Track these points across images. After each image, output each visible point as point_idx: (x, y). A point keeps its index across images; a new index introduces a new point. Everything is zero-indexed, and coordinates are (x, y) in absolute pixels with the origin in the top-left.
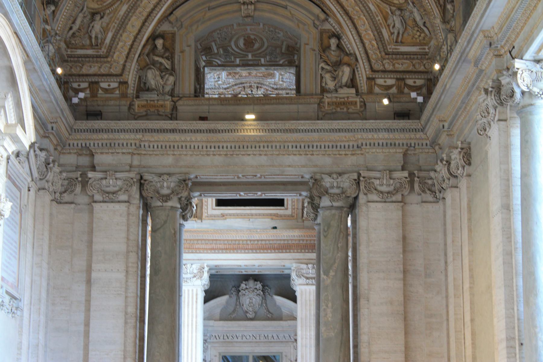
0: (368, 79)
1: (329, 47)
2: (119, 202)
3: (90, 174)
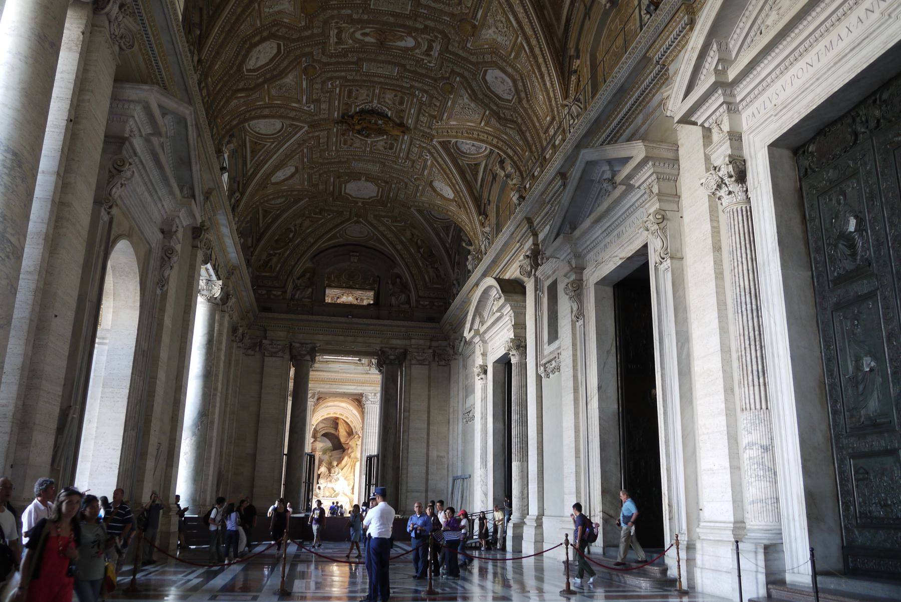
0: (416, 301)
2: (278, 357)
3: (264, 341)
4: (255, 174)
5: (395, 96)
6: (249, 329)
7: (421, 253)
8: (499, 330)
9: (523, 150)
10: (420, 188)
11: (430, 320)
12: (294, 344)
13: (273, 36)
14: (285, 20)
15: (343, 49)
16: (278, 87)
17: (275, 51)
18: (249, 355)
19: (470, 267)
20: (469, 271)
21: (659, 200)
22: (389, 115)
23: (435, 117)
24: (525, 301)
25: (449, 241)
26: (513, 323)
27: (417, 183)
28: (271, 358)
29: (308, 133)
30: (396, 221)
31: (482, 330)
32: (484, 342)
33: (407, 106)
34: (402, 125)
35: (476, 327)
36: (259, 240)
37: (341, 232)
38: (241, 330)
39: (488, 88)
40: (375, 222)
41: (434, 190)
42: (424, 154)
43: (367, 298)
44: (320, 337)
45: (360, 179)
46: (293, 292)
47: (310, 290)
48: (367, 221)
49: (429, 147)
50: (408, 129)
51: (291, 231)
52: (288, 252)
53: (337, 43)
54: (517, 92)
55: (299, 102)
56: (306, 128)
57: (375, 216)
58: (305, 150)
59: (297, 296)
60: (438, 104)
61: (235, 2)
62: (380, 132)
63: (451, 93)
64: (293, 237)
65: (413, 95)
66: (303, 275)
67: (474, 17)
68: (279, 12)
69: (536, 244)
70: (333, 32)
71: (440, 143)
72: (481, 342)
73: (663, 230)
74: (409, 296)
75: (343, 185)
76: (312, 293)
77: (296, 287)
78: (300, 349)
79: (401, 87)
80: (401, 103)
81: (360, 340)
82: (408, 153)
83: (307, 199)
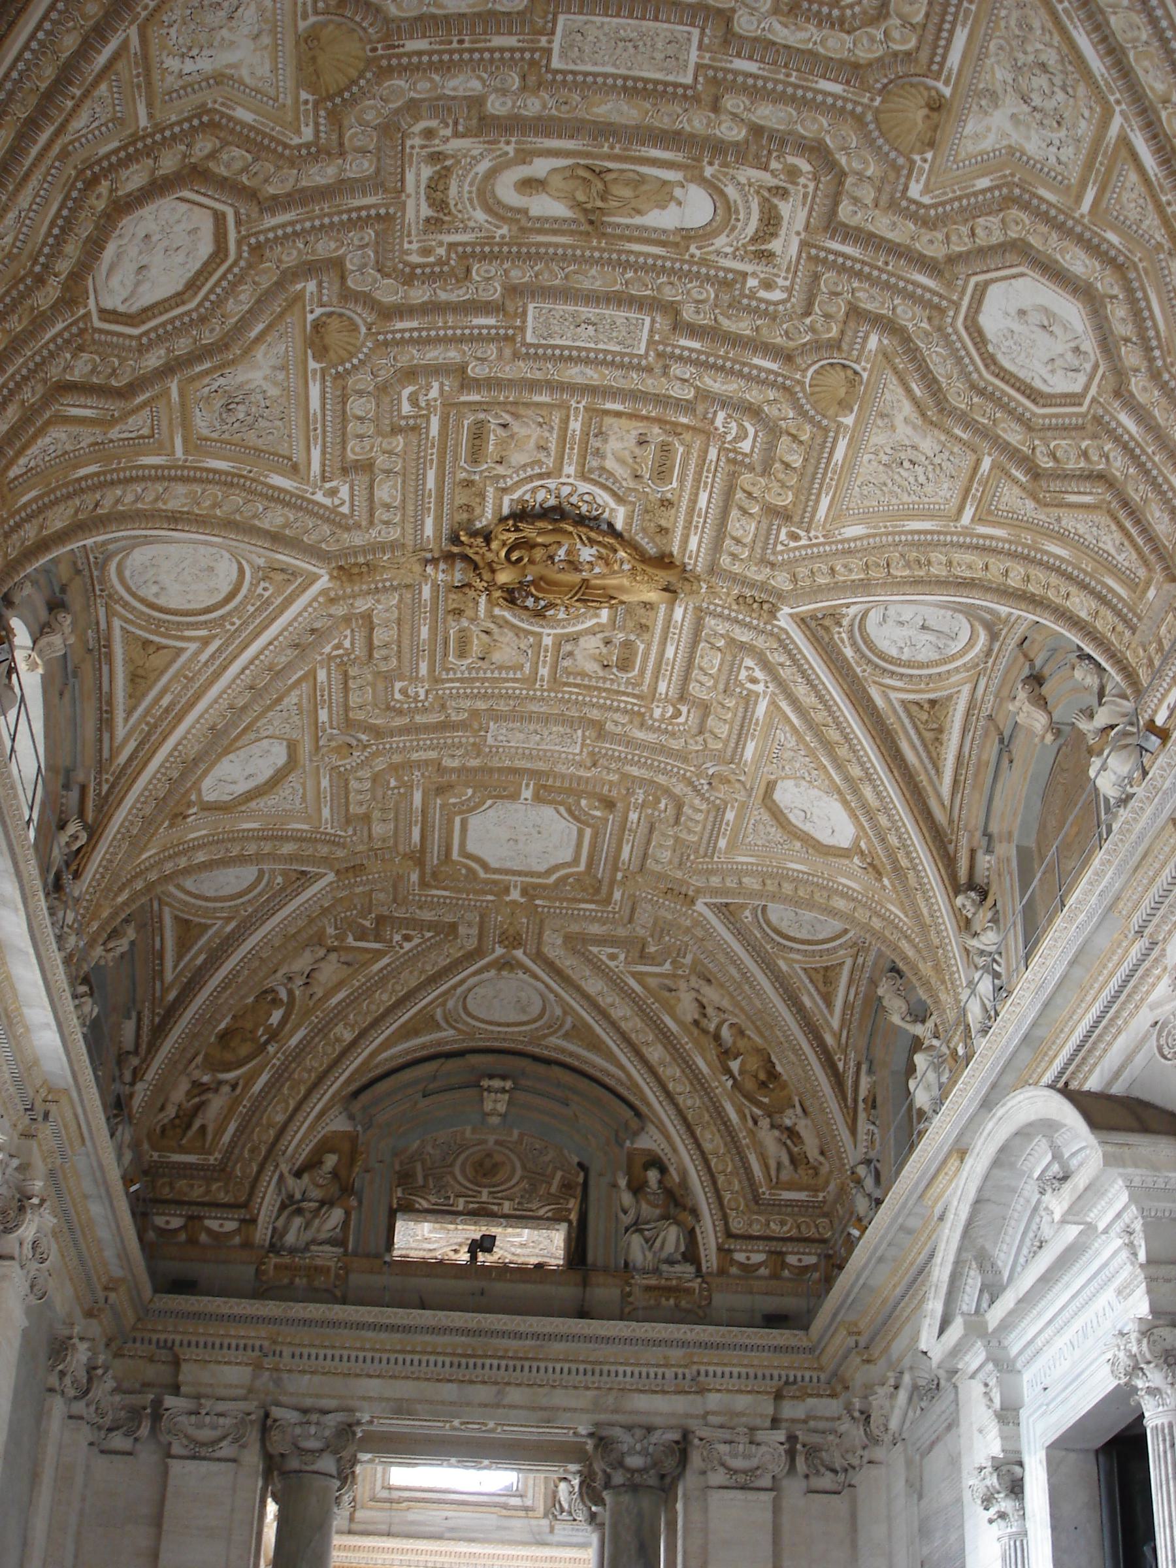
0: (720, 1249)
1: (645, 1183)
2: (219, 1460)
3: (170, 1401)
4: (139, 760)
5: (642, 442)
6: (117, 1355)
7: (732, 1076)
8: (1073, 1307)
9: (1132, 584)
10: (730, 815)
11: (774, 1320)
12: (276, 1412)
14: (242, 114)
15: (452, 246)
16: (218, 403)
17: (206, 248)
19: (922, 1098)
20: (921, 1113)
22: (619, 526)
23: (785, 515)
25: (835, 1023)
26: (1142, 1256)
27: (722, 792)
28: (191, 1465)
29: (332, 601)
30: (643, 957)
32: (1005, 1366)
33: (682, 481)
34: (664, 561)
36: (160, 1031)
37: (450, 1004)
38: (81, 1355)
39: (990, 361)
40: (567, 962)
41: (778, 815)
42: (743, 674)
44: (373, 1386)
45: (514, 797)
46: (280, 1223)
47: (337, 1214)
48: (539, 957)
49: (760, 642)
50: (685, 574)
51: (276, 1002)
52: (264, 1078)
53: (433, 224)
54: (1107, 343)
55: (294, 470)
56: (324, 582)
57: (568, 939)
58: (322, 675)
59: (290, 1239)
60: (796, 461)
61: (52, 7)
63: (844, 405)
65: (707, 433)
66: (311, 1165)
67: (935, 67)
68: (218, 79)
70: (418, 176)
71: (802, 621)
72: (990, 1366)
74: (692, 1233)
75: (458, 820)
76: (346, 1224)
77: (290, 1205)
78: (298, 1430)
79: (661, 400)
80: (662, 473)
81: (515, 1395)
82: (686, 679)
83: (331, 877)
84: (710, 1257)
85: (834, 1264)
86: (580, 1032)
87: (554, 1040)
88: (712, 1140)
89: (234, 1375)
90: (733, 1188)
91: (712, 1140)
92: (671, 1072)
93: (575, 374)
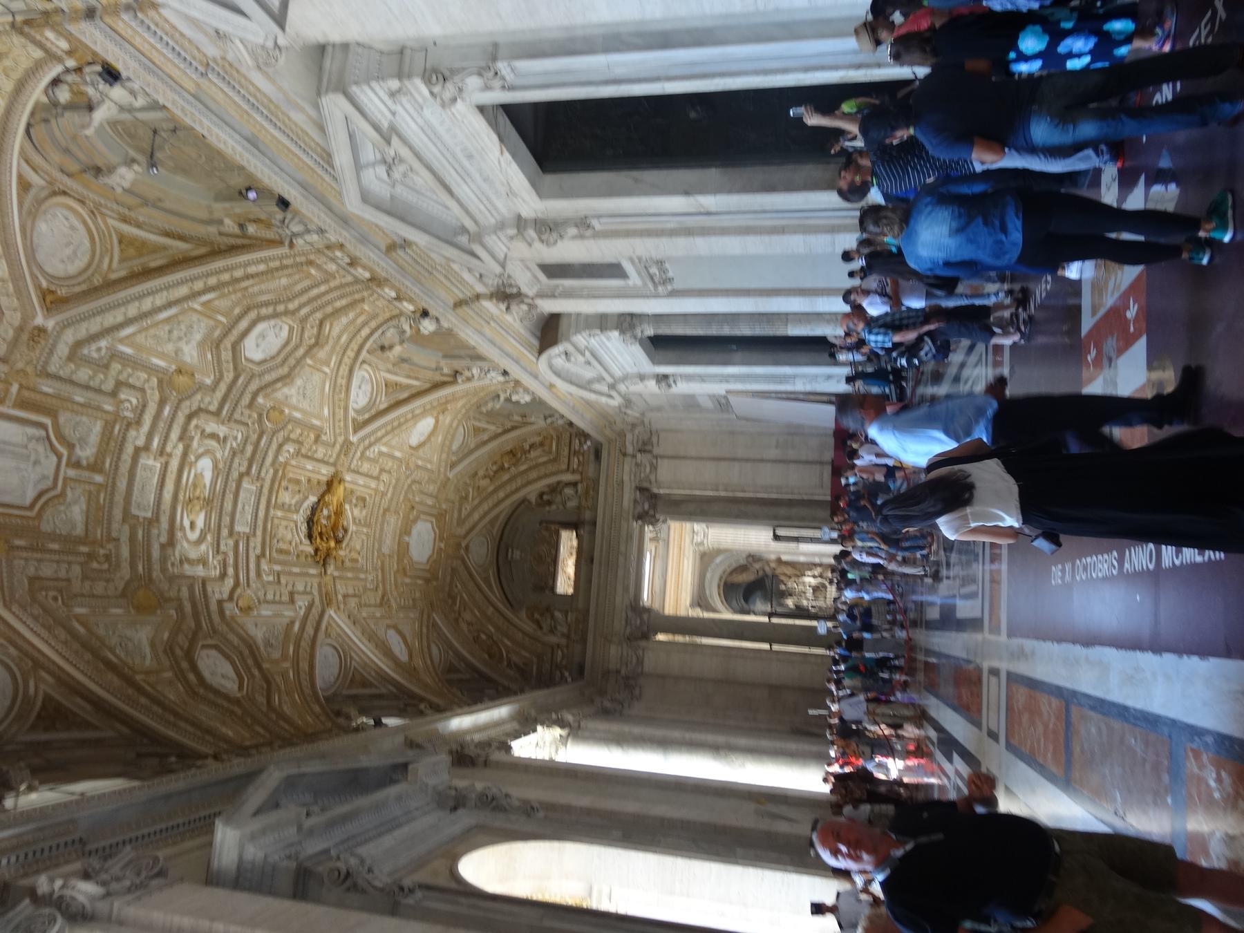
9: (361, 314)
10: (420, 463)
13: (190, 656)
14: (166, 635)
16: (269, 649)
17: (214, 653)
18: (640, 694)
19: (527, 398)
21: (410, 76)
24: (569, 315)
27: (412, 466)
29: (339, 608)
30: (466, 498)
31: (610, 380)
32: (625, 378)
34: (330, 484)
35: (605, 389)
38: (607, 704)
39: (273, 358)
40: (467, 526)
41: (421, 445)
43: (568, 542)
44: (618, 600)
45: (408, 544)
49: (361, 447)
52: (506, 641)
54: (275, 315)
58: (364, 614)
60: (298, 431)
62: (339, 513)
63: (282, 412)
64: (486, 634)
65: (286, 464)
66: (538, 623)
67: (164, 371)
68: (153, 645)
69: (491, 296)
71: (355, 431)
73: (453, 72)
77: (552, 631)
79: (273, 481)
80: (298, 482)
81: (622, 548)
82: (371, 477)
84: (576, 477)
85: (584, 435)
86: (492, 522)
87: (495, 532)
88: (533, 475)
89: (614, 650)
90: (550, 468)
91: (533, 475)
92: (508, 489)
93: (261, 514)
